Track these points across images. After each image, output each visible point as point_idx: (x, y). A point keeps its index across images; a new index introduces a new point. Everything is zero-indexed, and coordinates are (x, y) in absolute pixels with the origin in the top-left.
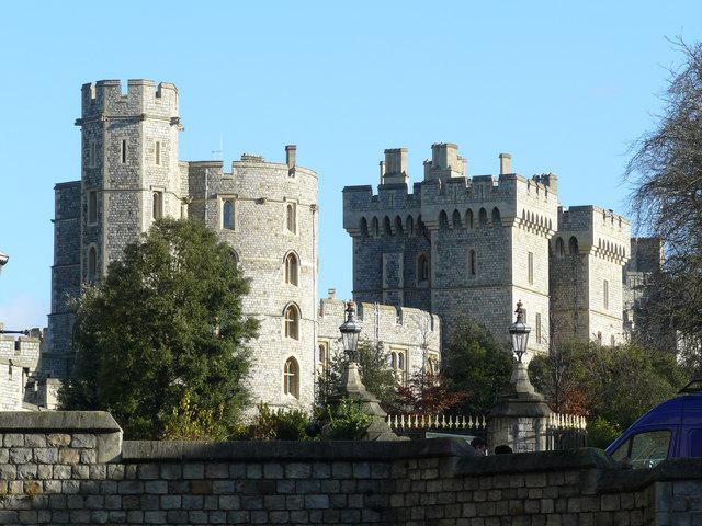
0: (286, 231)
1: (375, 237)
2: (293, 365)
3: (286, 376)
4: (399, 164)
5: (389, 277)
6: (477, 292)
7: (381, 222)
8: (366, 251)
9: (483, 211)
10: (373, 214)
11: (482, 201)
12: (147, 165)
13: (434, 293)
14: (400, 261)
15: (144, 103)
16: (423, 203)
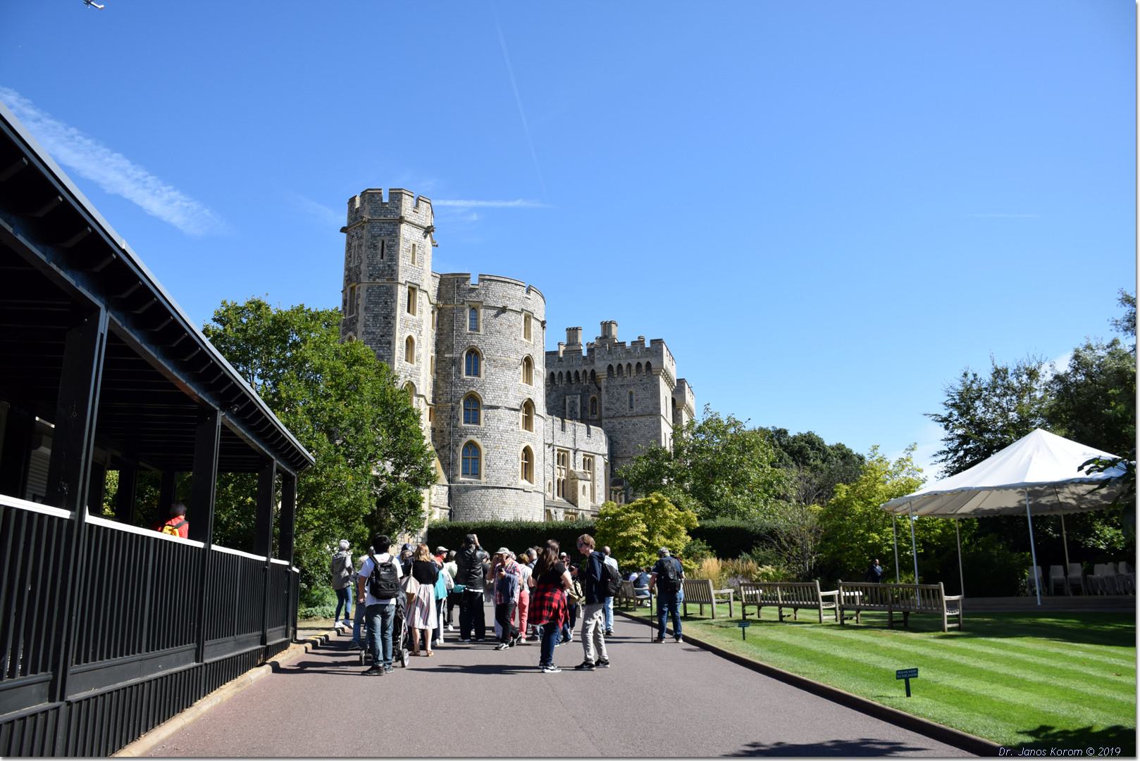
0: (523, 339)
1: (560, 385)
2: (527, 453)
3: (522, 463)
5: (571, 411)
6: (635, 420)
7: (564, 375)
8: (554, 395)
9: (639, 365)
10: (559, 370)
11: (638, 357)
12: (404, 261)
13: (604, 421)
14: (578, 401)
15: (403, 208)
16: (596, 361)
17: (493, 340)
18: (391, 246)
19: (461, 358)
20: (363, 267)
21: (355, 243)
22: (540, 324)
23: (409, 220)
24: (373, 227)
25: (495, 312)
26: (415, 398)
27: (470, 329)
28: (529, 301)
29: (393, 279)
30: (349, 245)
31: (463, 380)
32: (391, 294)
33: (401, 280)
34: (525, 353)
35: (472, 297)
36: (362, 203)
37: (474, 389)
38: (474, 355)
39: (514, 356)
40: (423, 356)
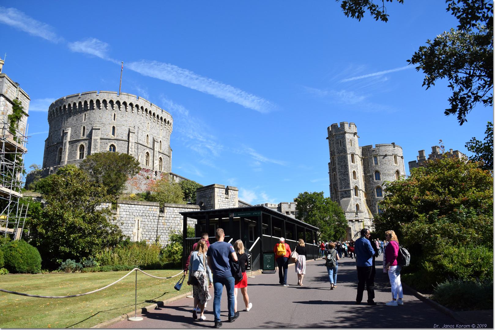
0: (395, 164)
4: (423, 154)
12: (348, 146)
15: (345, 128)
17: (383, 167)
18: (344, 142)
19: (373, 175)
20: (335, 150)
21: (332, 142)
22: (400, 158)
23: (348, 132)
24: (336, 137)
25: (383, 157)
26: (358, 191)
27: (375, 164)
28: (395, 151)
29: (346, 153)
30: (330, 143)
31: (375, 182)
32: (346, 158)
33: (348, 152)
34: (396, 169)
35: (374, 153)
36: (332, 129)
37: (379, 185)
38: (378, 173)
39: (392, 171)
40: (359, 177)
